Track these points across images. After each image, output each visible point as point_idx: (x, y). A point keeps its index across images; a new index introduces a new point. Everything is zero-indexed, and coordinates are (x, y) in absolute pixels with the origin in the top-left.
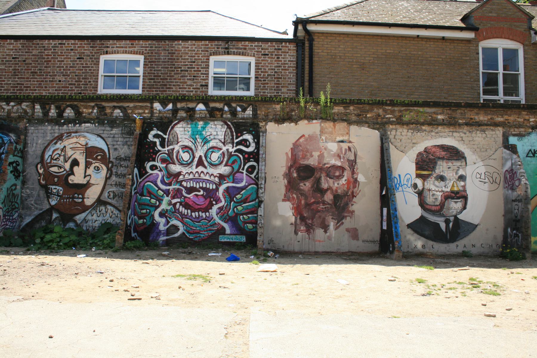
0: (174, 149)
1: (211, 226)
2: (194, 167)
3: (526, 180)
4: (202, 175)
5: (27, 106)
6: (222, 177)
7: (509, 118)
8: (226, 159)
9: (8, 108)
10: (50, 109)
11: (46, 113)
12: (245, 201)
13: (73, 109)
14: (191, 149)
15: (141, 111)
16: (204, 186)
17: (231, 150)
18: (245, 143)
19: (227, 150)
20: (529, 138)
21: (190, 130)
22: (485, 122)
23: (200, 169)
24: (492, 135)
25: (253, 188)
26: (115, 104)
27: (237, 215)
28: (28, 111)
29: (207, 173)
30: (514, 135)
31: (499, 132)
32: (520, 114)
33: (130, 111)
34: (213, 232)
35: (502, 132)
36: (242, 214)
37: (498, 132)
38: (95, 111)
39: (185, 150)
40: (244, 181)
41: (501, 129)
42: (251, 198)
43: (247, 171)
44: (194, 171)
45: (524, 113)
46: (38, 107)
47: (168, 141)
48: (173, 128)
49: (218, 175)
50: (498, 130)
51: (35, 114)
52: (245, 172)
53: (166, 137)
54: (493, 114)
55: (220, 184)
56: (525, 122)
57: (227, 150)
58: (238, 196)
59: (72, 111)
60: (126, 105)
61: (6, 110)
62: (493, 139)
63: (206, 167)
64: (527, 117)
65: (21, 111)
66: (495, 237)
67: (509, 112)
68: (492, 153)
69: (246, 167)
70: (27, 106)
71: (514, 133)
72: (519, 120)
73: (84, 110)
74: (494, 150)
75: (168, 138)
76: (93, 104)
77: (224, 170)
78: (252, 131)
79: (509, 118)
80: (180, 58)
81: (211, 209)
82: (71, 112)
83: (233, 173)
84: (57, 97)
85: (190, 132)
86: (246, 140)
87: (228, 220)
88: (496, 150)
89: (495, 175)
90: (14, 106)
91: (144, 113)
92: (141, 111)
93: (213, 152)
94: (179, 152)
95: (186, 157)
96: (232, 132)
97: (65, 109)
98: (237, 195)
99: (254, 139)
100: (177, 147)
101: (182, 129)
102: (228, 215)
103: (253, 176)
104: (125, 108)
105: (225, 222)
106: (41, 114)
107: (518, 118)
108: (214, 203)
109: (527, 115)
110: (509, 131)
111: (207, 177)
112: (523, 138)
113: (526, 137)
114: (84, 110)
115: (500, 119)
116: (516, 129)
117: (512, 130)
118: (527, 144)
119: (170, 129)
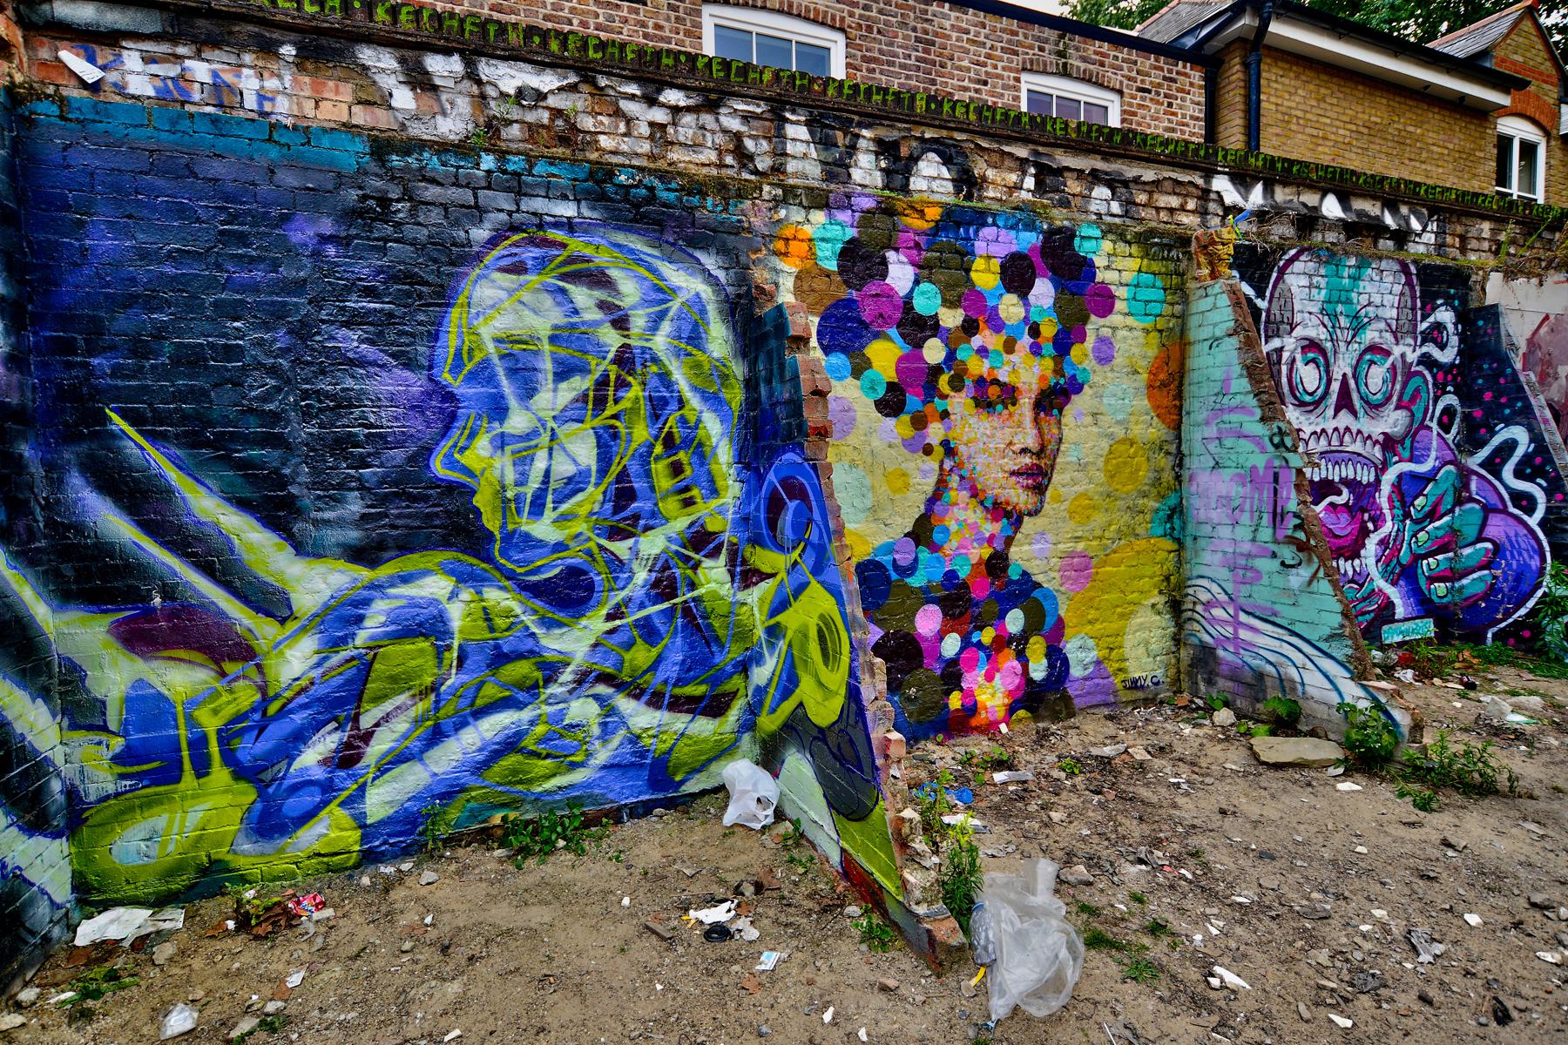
0: (1280, 350)
1: (1364, 599)
2: (1330, 412)
4: (1347, 438)
5: (747, 118)
6: (1389, 444)
8: (1398, 387)
9: (660, 116)
10: (852, 149)
11: (837, 170)
12: (1433, 515)
13: (947, 161)
14: (1323, 352)
15: (1174, 202)
16: (1351, 476)
17: (1412, 357)
18: (1435, 335)
19: (1403, 356)
21: (1323, 282)
23: (1345, 419)
25: (1448, 472)
26: (1100, 165)
27: (1417, 558)
28: (749, 144)
29: (1359, 432)
33: (1142, 198)
34: (1368, 617)
36: (1425, 556)
38: (1030, 182)
39: (1311, 355)
40: (1433, 454)
42: (1444, 508)
43: (1440, 423)
44: (1329, 428)
46: (797, 132)
47: (1268, 321)
48: (1282, 272)
49: (1381, 438)
51: (792, 166)
52: (1434, 425)
53: (1262, 304)
55: (1382, 468)
57: (1403, 356)
58: (1420, 501)
59: (944, 170)
60: (1130, 171)
61: (645, 130)
63: (1354, 413)
65: (720, 139)
69: (1437, 413)
70: (747, 118)
73: (990, 173)
75: (1268, 311)
76: (1022, 152)
77: (1393, 421)
78: (1453, 297)
80: (949, 63)
81: (1363, 546)
82: (939, 178)
83: (1416, 429)
84: (876, 98)
85: (1323, 292)
86: (1439, 326)
87: (1399, 575)
90: (688, 109)
91: (1183, 209)
92: (1174, 202)
93: (1372, 362)
94: (1294, 360)
95: (1309, 377)
96: (1413, 297)
97: (914, 159)
98: (1416, 498)
99: (1455, 325)
100: (1290, 343)
101: (1304, 281)
102: (1399, 562)
103: (1449, 437)
104: (1125, 183)
105: (1394, 583)
106: (814, 171)
108: (1370, 526)
111: (1357, 447)
114: (990, 173)
119: (1274, 275)
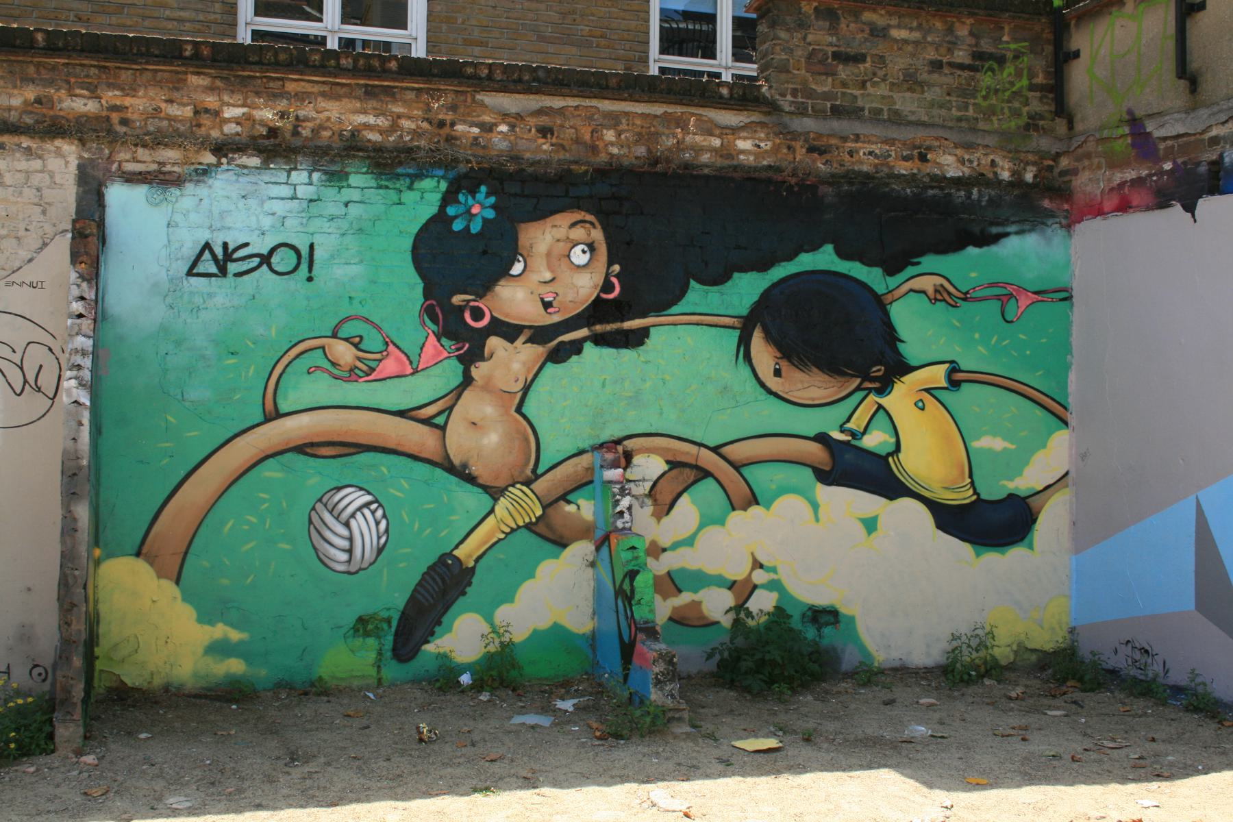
3: (81, 384)
7: (128, 101)
20: (202, 191)
22: (13, 117)
24: (28, 173)
30: (132, 178)
31: (62, 162)
32: (177, 84)
35: (73, 162)
37: (54, 163)
41: (70, 149)
45: (194, 80)
50: (59, 153)
54: (51, 83)
56: (206, 120)
62: (29, 193)
64: (211, 101)
66: (25, 635)
67: (126, 76)
68: (24, 254)
71: (130, 167)
72: (174, 110)
74: (33, 241)
79: (128, 101)
88: (45, 245)
89: (37, 355)
107: (171, 101)
109: (211, 89)
110: (110, 159)
112: (175, 191)
113: (189, 187)
115: (81, 105)
116: (141, 153)
117: (123, 155)
118: (193, 217)
